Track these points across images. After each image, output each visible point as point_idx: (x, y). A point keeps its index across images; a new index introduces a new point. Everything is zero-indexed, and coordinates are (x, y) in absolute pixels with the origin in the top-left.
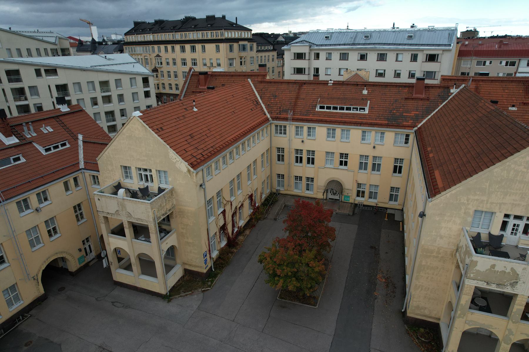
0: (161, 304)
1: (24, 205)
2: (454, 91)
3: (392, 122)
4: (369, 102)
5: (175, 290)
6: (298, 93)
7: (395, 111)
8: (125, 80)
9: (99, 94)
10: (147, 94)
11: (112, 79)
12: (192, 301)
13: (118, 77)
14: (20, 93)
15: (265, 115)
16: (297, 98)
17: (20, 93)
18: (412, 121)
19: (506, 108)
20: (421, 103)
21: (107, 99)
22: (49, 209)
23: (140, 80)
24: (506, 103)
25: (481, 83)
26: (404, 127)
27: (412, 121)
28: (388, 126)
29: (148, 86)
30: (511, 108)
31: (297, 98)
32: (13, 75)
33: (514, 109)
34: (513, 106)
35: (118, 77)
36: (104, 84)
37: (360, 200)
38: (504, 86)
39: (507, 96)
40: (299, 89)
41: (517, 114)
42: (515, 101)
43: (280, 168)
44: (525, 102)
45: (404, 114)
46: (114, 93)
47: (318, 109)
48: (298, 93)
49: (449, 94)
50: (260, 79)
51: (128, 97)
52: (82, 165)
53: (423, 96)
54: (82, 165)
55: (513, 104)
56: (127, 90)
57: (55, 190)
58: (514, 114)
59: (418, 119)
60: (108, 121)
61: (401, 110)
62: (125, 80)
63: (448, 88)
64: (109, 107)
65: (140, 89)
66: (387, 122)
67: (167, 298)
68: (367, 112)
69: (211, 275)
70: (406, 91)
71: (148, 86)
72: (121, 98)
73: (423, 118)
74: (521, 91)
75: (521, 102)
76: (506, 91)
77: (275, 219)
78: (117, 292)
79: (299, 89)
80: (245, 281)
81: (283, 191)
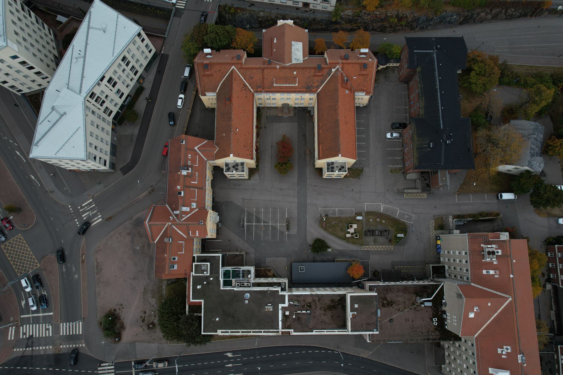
0: (249, 181)
2: (333, 70)
3: (308, 90)
5: (250, 176)
6: (263, 75)
8: (132, 46)
10: (143, 40)
12: (256, 177)
16: (263, 79)
20: (319, 78)
23: (137, 39)
31: (263, 79)
36: (124, 59)
37: (297, 106)
40: (263, 72)
43: (260, 102)
47: (275, 85)
48: (263, 75)
50: (240, 66)
52: (206, 160)
53: (319, 74)
54: (206, 160)
59: (318, 87)
63: (331, 69)
67: (249, 179)
68: (297, 85)
69: (257, 166)
73: (320, 86)
77: (265, 127)
78: (232, 182)
79: (263, 72)
80: (268, 165)
81: (261, 106)
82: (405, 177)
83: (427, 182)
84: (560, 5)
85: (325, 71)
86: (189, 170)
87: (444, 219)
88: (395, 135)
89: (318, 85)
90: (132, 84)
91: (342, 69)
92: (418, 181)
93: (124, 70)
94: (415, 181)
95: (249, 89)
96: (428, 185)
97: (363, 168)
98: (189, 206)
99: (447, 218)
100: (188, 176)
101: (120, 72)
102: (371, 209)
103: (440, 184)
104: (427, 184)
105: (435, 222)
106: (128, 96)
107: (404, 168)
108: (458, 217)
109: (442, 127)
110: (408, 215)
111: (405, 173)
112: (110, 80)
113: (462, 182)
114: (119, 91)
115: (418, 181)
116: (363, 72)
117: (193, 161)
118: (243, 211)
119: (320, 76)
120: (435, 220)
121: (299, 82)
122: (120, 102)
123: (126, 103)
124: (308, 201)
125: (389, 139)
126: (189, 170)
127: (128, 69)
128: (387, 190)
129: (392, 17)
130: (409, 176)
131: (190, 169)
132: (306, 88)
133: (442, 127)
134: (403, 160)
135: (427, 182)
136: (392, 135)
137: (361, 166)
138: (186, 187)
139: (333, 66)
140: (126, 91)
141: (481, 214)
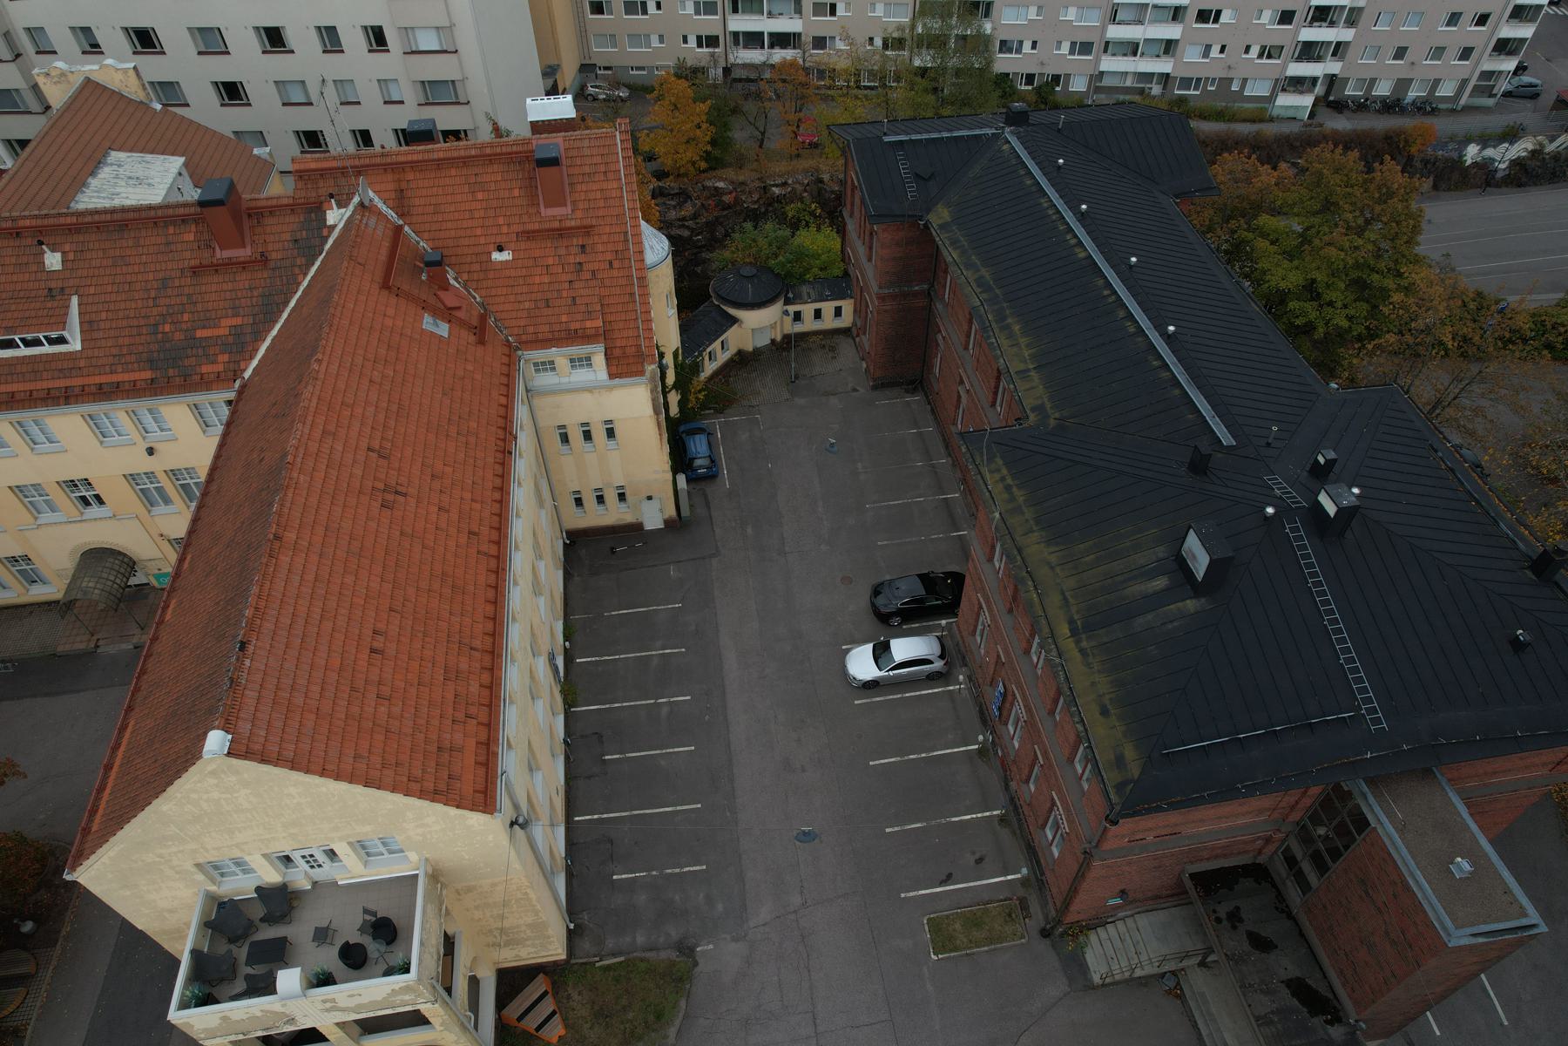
2: (335, 216)
3: (166, 370)
4: (75, 300)
7: (167, 328)
18: (226, 357)
19: (484, 258)
24: (482, 240)
25: (410, 176)
26: (205, 384)
27: (226, 357)
28: (157, 387)
30: (497, 256)
33: (505, 256)
34: (500, 249)
38: (473, 180)
39: (482, 213)
41: (513, 273)
42: (505, 229)
44: (530, 227)
45: (199, 334)
49: (322, 229)
53: (244, 253)
55: (499, 239)
58: (507, 273)
59: (241, 346)
61: (186, 317)
63: (318, 210)
66: (148, 375)
68: (76, 345)
70: (191, 237)
73: (259, 337)
74: (516, 192)
75: (520, 228)
76: (480, 196)
82: (1076, 966)
83: (1285, 965)
84: (1468, 140)
85: (279, 235)
88: (904, 648)
89: (237, 332)
91: (401, 203)
92: (1198, 982)
94: (1170, 985)
96: (1318, 1003)
97: (686, 950)
103: (1459, 938)
104: (1298, 988)
107: (1037, 880)
109: (1227, 439)
111: (1064, 933)
115: (1198, 982)
119: (244, 265)
121: (88, 326)
125: (871, 686)
129: (793, 197)
130: (1104, 954)
132: (152, 363)
133: (1227, 439)
134: (1019, 823)
135: (1285, 965)
136: (881, 652)
137: (674, 932)
139: (325, 187)
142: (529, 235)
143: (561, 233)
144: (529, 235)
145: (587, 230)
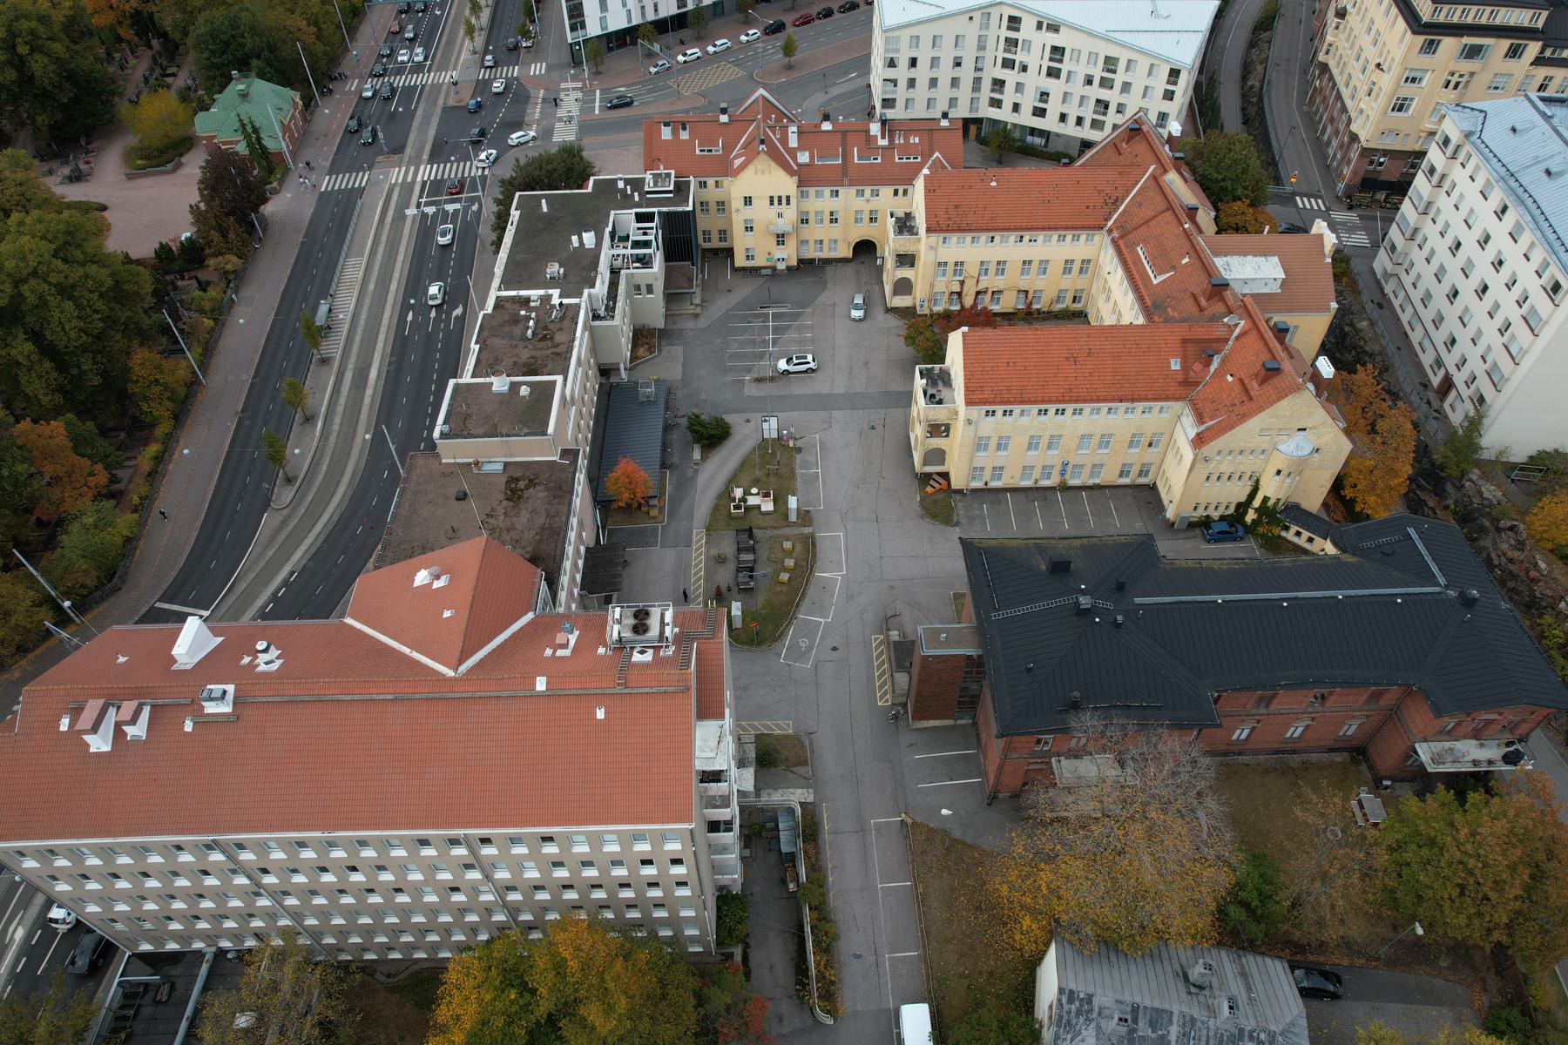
0: (882, 310)
1: (861, 193)
8: (1143, 64)
9: (1098, 73)
10: (1169, 95)
11: (1124, 57)
13: (1133, 56)
14: (1012, 44)
15: (1107, 220)
17: (1012, 44)
21: (1106, 83)
22: (875, 203)
29: (1175, 83)
32: (1014, 22)
35: (1133, 56)
36: (1110, 63)
46: (1119, 78)
51: (1137, 90)
56: (1138, 79)
57: (886, 191)
60: (1095, 112)
62: (1143, 64)
64: (1104, 94)
65: (1160, 83)
68: (1155, 282)
71: (1175, 83)
72: (1126, 87)
86: (883, 137)
87: (801, 770)
90: (1070, 129)
93: (1089, 82)
95: (1110, 215)
97: (957, 524)
98: (802, 147)
99: (807, 782)
100: (870, 139)
101: (1082, 70)
102: (824, 551)
105: (786, 737)
106: (1044, 134)
108: (810, 830)
110: (809, 649)
112: (1058, 52)
113: (957, 834)
114: (1044, 96)
116: (1254, 386)
117: (906, 149)
118: (804, 305)
120: (795, 740)
122: (1026, 119)
123: (1029, 139)
124: (837, 414)
126: (883, 137)
127: (1096, 92)
128: (892, 588)
131: (885, 142)
132: (1154, 304)
138: (843, 134)
140: (1049, 123)
141: (822, 914)
142: (1241, 381)
143: (1247, 391)
144: (1241, 381)
145: (1251, 399)
